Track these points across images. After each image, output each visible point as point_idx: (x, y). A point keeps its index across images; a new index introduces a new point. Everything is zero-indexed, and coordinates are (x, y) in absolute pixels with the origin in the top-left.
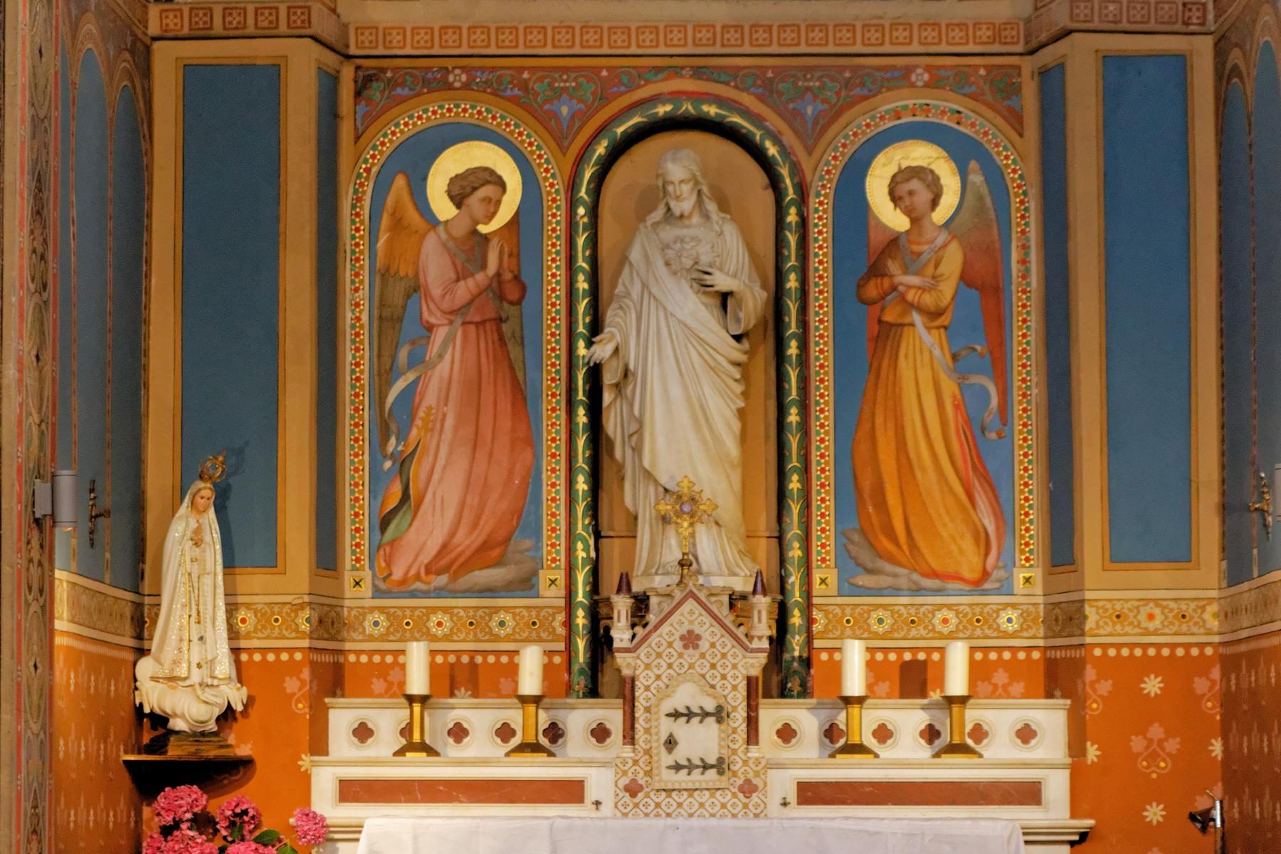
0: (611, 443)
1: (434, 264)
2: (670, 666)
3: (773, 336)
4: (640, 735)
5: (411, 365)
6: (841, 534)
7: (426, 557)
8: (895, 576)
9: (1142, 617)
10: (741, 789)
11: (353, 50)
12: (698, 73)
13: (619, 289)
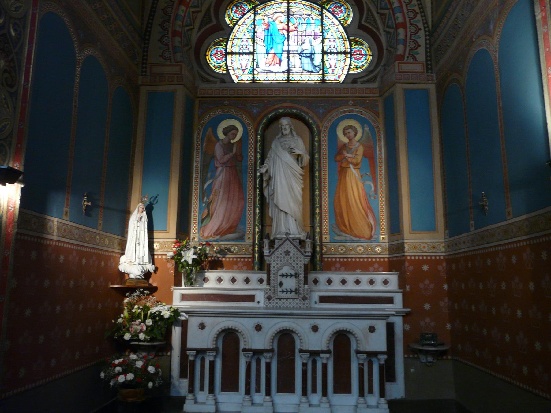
0: (265, 198)
1: (218, 150)
2: (281, 261)
3: (311, 172)
4: (272, 282)
5: (211, 178)
6: (331, 225)
7: (214, 231)
8: (346, 237)
9: (422, 247)
10: (303, 299)
11: (198, 95)
12: (291, 101)
13: (268, 156)
